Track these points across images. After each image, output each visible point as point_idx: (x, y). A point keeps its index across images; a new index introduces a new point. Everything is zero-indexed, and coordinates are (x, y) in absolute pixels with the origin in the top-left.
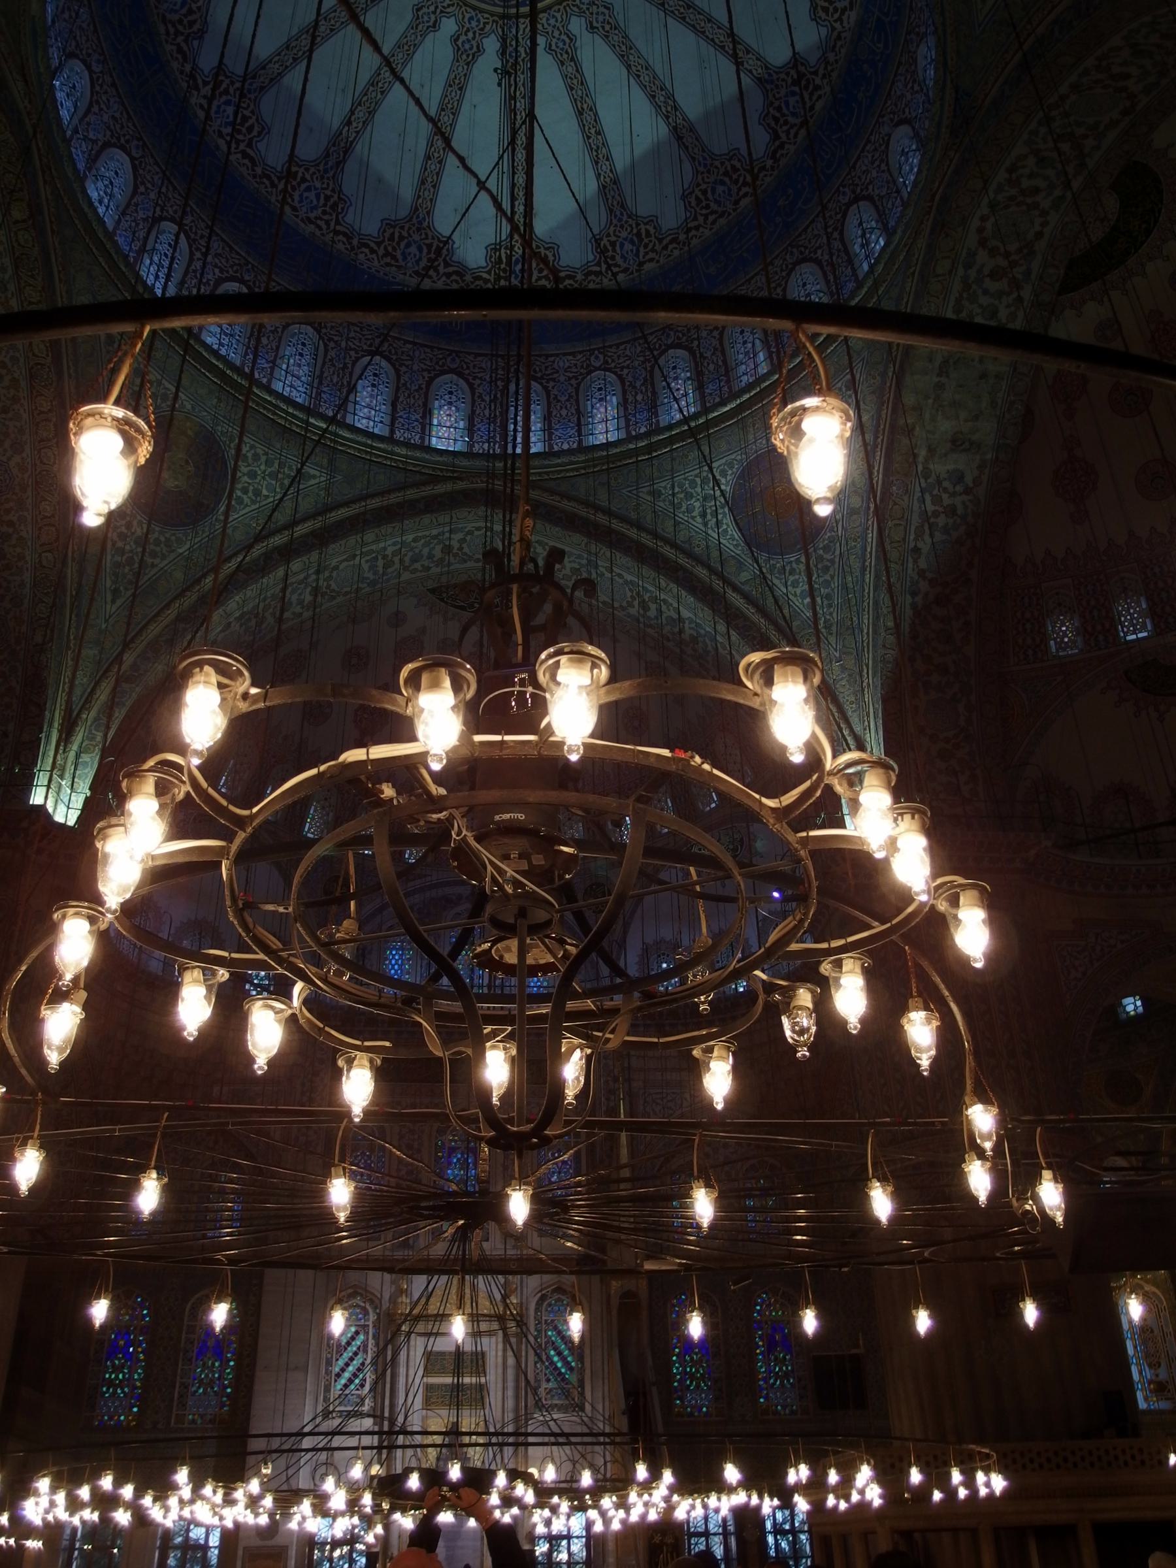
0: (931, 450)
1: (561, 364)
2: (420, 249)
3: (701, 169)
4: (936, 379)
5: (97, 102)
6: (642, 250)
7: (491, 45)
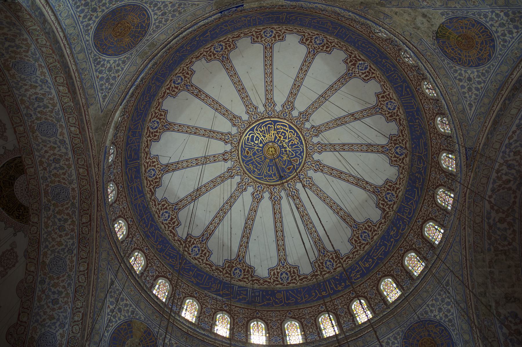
0: (497, 303)
1: (306, 311)
2: (240, 271)
3: (355, 229)
4: (489, 270)
5: (119, 201)
6: (335, 263)
7: (266, 195)
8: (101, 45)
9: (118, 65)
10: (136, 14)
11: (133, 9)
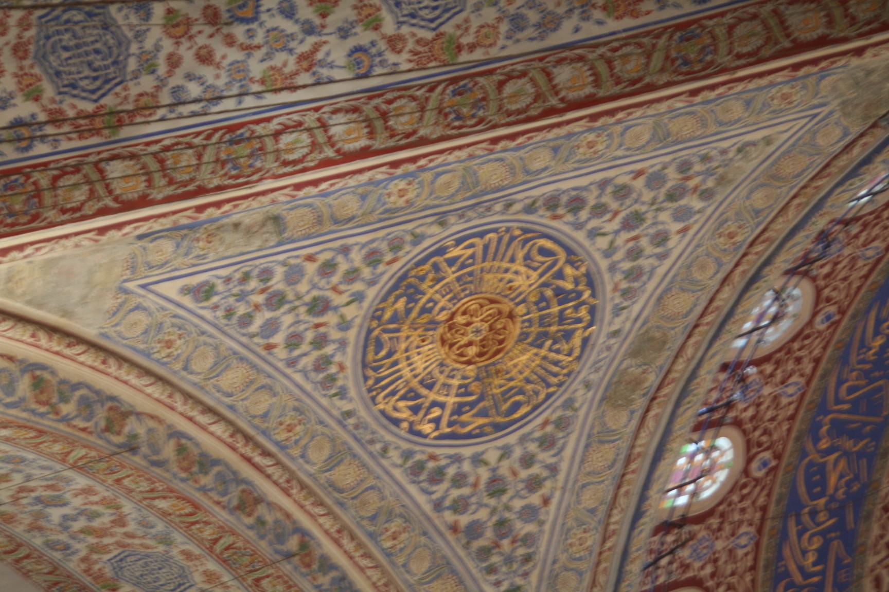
8: (415, 410)
9: (528, 461)
10: (512, 260)
11: (486, 247)
